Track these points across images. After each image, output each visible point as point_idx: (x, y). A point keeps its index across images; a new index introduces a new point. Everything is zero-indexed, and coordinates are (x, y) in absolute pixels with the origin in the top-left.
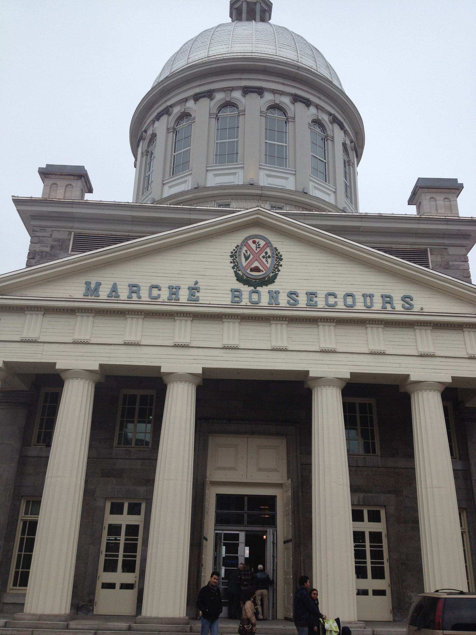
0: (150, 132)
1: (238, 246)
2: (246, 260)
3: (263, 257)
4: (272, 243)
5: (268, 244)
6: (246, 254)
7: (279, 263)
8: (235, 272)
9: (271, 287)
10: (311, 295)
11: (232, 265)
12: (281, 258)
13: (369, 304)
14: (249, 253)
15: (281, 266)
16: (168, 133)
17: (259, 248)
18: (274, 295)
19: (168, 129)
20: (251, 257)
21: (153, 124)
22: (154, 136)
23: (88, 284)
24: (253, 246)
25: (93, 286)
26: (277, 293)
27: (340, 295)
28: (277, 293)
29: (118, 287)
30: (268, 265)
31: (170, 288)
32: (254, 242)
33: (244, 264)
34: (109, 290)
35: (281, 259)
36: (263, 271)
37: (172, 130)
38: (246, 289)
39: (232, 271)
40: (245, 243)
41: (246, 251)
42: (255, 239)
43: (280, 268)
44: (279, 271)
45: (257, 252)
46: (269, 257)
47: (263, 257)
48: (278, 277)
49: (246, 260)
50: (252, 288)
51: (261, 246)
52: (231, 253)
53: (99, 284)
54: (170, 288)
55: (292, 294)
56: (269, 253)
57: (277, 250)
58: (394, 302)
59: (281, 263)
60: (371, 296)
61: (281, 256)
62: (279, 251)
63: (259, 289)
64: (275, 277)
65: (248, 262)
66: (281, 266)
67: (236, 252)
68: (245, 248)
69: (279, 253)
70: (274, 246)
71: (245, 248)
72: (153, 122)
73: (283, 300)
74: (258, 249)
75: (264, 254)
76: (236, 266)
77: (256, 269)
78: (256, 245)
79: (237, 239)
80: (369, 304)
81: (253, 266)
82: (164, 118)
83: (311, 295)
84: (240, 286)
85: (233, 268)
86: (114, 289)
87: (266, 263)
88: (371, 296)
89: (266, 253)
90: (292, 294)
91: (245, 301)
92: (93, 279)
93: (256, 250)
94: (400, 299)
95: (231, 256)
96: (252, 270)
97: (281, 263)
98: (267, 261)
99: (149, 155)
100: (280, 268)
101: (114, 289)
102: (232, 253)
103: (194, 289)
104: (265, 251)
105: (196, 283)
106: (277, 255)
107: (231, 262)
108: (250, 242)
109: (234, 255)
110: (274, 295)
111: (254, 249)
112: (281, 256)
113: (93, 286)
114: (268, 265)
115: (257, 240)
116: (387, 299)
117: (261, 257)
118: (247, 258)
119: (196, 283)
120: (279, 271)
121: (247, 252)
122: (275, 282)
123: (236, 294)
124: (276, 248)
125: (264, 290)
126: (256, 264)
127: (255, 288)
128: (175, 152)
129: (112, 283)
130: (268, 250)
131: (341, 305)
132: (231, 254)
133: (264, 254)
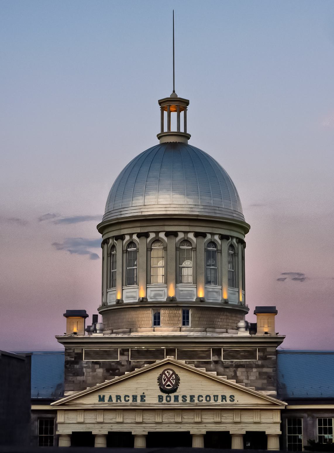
1: (161, 374)
2: (164, 381)
3: (172, 379)
4: (176, 372)
5: (174, 373)
7: (179, 382)
8: (160, 387)
10: (192, 397)
13: (216, 400)
17: (170, 375)
18: (176, 398)
20: (167, 379)
23: (100, 396)
24: (167, 374)
25: (102, 397)
27: (204, 396)
29: (112, 397)
30: (174, 383)
31: (133, 396)
32: (168, 372)
33: (164, 383)
34: (108, 399)
38: (164, 395)
39: (158, 387)
40: (163, 373)
41: (164, 377)
42: (168, 371)
45: (169, 377)
46: (174, 379)
47: (172, 379)
49: (164, 381)
50: (167, 395)
51: (171, 374)
53: (104, 396)
54: (133, 396)
55: (184, 397)
56: (174, 378)
57: (178, 375)
58: (227, 398)
60: (217, 396)
61: (179, 378)
63: (170, 395)
64: (177, 388)
65: (165, 382)
67: (160, 377)
68: (164, 375)
69: (178, 377)
70: (176, 373)
71: (164, 375)
73: (180, 399)
74: (169, 376)
75: (172, 378)
76: (160, 384)
77: (169, 386)
79: (160, 371)
80: (216, 400)
83: (192, 397)
84: (161, 394)
85: (159, 385)
86: (110, 398)
87: (173, 382)
88: (217, 396)
89: (173, 377)
90: (184, 397)
91: (164, 401)
92: (102, 394)
94: (229, 396)
95: (158, 379)
98: (173, 381)
101: (110, 398)
102: (158, 378)
103: (143, 397)
105: (144, 393)
107: (158, 383)
108: (166, 372)
109: (160, 379)
110: (176, 398)
111: (168, 376)
113: (102, 397)
114: (174, 383)
115: (169, 371)
117: (171, 379)
118: (165, 380)
119: (144, 393)
120: (178, 386)
121: (165, 377)
123: (160, 398)
124: (177, 374)
125: (172, 395)
126: (169, 383)
129: (109, 395)
130: (174, 376)
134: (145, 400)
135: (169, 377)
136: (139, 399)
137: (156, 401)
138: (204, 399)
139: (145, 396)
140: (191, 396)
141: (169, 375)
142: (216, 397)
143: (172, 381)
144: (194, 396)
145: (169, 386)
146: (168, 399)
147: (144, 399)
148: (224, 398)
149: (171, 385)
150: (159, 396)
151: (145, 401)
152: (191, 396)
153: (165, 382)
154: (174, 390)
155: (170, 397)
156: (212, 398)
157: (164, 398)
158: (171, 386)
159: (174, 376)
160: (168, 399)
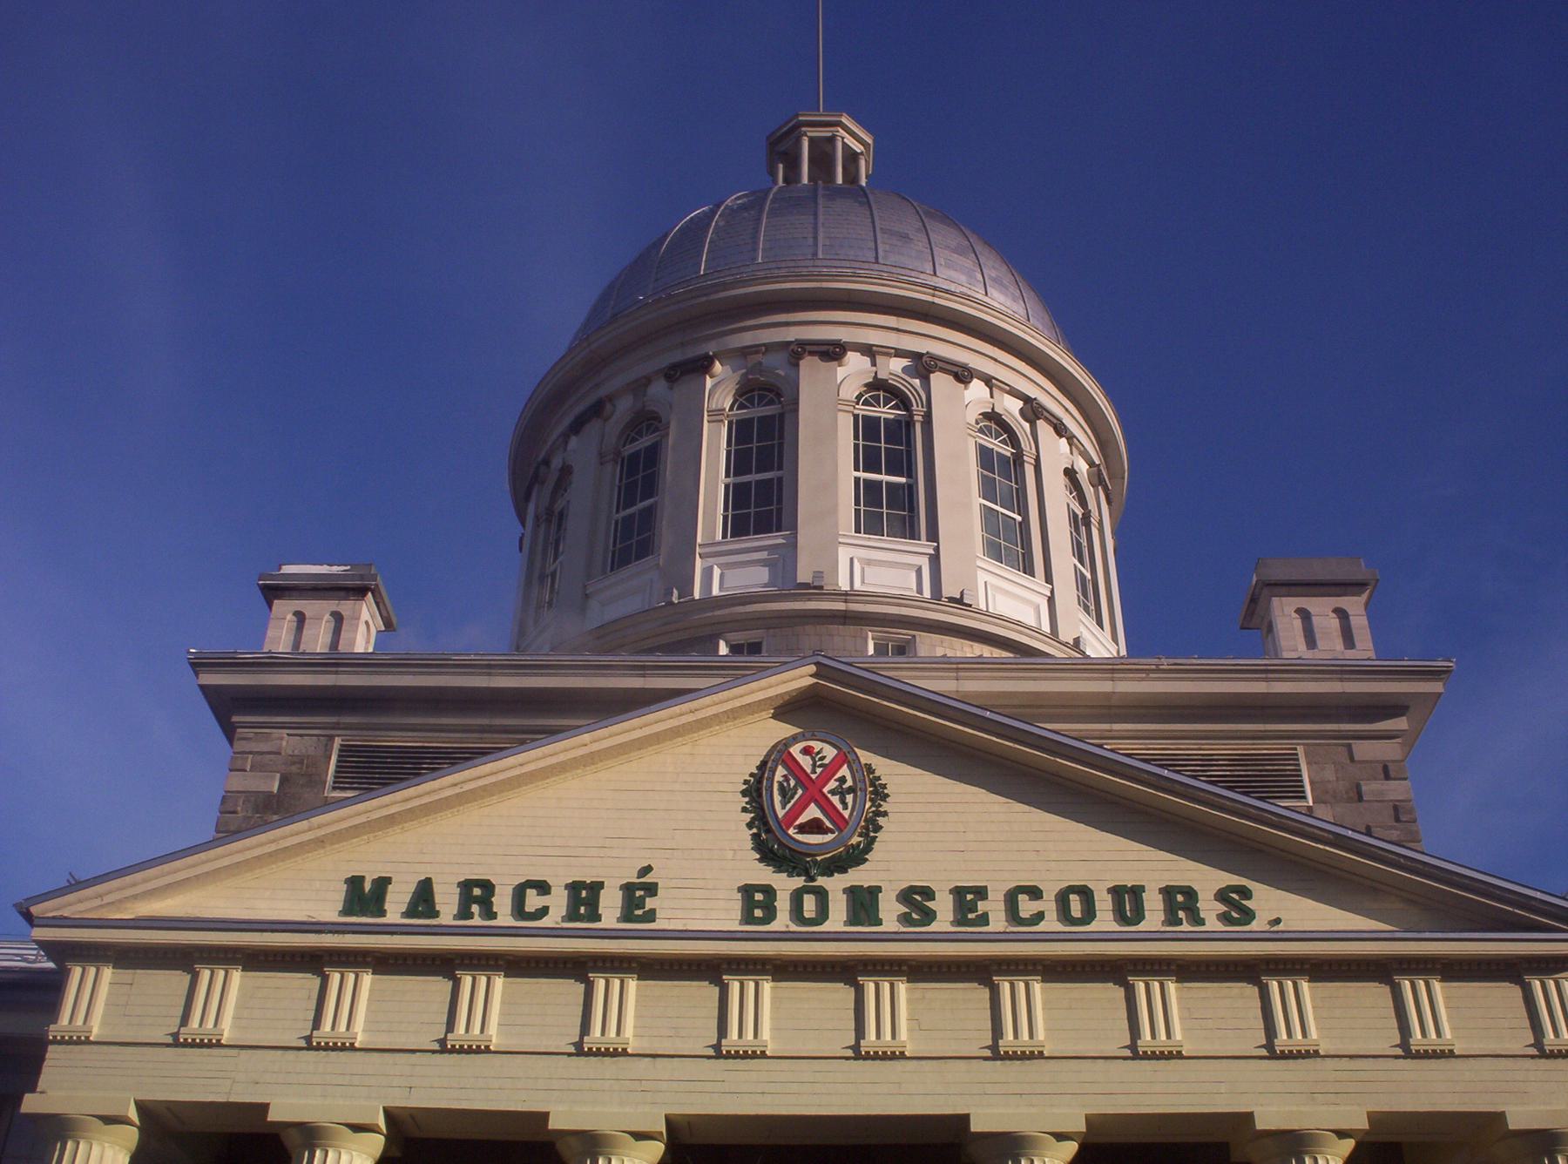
0: (556, 463)
3: (833, 792)
6: (785, 784)
8: (755, 837)
9: (857, 876)
11: (748, 817)
12: (886, 791)
14: (792, 783)
15: (885, 814)
16: (602, 464)
18: (863, 903)
19: (601, 455)
21: (567, 443)
22: (566, 471)
24: (805, 762)
26: (874, 891)
28: (874, 891)
30: (846, 814)
31: (574, 888)
32: (807, 751)
35: (885, 797)
36: (833, 832)
37: (612, 456)
38: (785, 884)
39: (746, 835)
42: (811, 743)
43: (881, 820)
44: (878, 828)
46: (851, 790)
48: (876, 846)
50: (799, 882)
52: (744, 784)
56: (849, 783)
59: (885, 807)
61: (884, 786)
62: (877, 774)
63: (821, 881)
65: (789, 806)
66: (885, 814)
68: (780, 772)
72: (566, 437)
73: (890, 911)
75: (833, 784)
76: (760, 818)
77: (814, 827)
78: (813, 759)
81: (802, 819)
82: (593, 428)
83: (967, 899)
84: (764, 875)
85: (750, 825)
87: (840, 807)
88: (1136, 892)
89: (843, 780)
90: (917, 900)
93: (814, 772)
96: (803, 829)
97: (885, 807)
99: (555, 520)
100: (881, 820)
102: (746, 782)
104: (839, 775)
106: (872, 784)
107: (744, 810)
108: (795, 750)
109: (755, 791)
110: (863, 903)
112: (884, 786)
116: (1180, 901)
118: (786, 794)
120: (878, 828)
121: (787, 780)
122: (867, 860)
123: (756, 901)
125: (836, 885)
126: (813, 812)
127: (813, 879)
128: (617, 512)
130: (844, 771)
131: (1051, 924)
132: (745, 787)
133: (833, 784)
134: (653, 911)
135: (814, 776)
136: (610, 907)
137: (728, 916)
138: (1048, 906)
139: (652, 889)
140: (959, 892)
141: (814, 765)
142: (1128, 900)
143: (835, 800)
144: (981, 893)
145: (814, 827)
146: (809, 903)
147: (650, 903)
148: (1180, 901)
149: (828, 824)
150: (747, 891)
151: (650, 916)
152: (959, 892)
153: (789, 806)
154: (854, 858)
155: (822, 895)
156: (1104, 903)
157: (783, 904)
158: (825, 831)
159: (844, 771)
160: (809, 903)
